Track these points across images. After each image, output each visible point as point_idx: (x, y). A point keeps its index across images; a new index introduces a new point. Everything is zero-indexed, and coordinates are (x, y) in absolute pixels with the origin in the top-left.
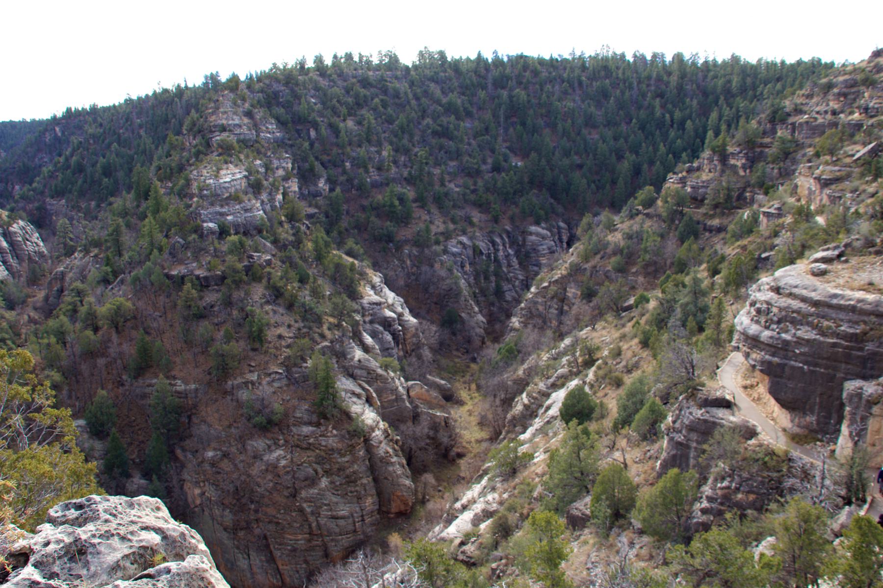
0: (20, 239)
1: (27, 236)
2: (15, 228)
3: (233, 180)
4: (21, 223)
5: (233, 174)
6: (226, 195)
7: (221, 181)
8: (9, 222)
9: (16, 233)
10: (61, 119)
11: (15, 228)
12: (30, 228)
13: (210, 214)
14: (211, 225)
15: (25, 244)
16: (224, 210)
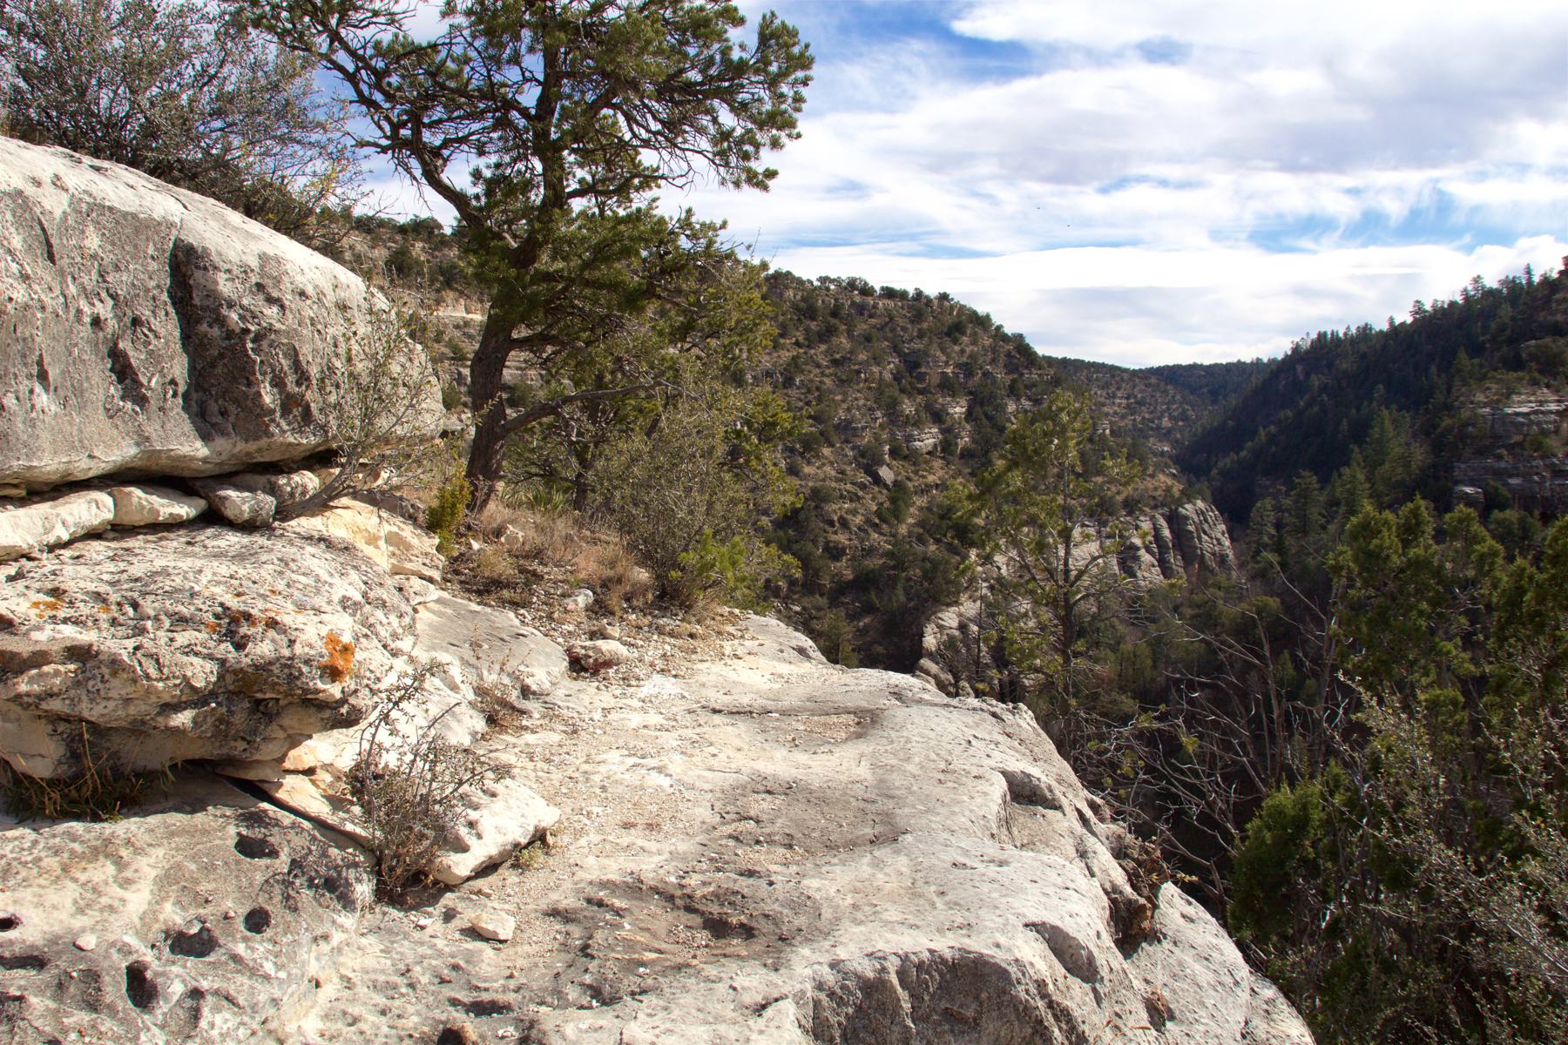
0: (1191, 528)
1: (1206, 527)
2: (1188, 509)
3: (1536, 412)
4: (1200, 504)
5: (1541, 403)
6: (1517, 438)
7: (1509, 411)
8: (1179, 500)
9: (1186, 518)
10: (1307, 352)
11: (1188, 509)
12: (1213, 514)
13: (1473, 469)
14: (1468, 490)
15: (1200, 538)
16: (1503, 465)
